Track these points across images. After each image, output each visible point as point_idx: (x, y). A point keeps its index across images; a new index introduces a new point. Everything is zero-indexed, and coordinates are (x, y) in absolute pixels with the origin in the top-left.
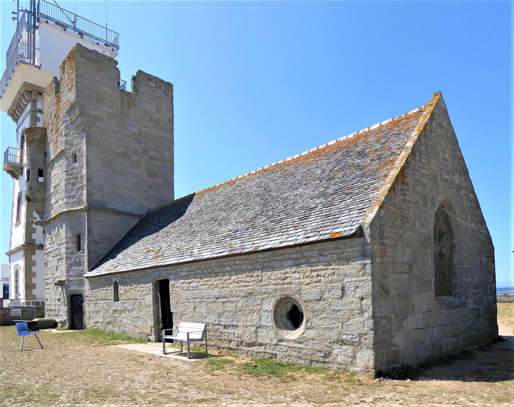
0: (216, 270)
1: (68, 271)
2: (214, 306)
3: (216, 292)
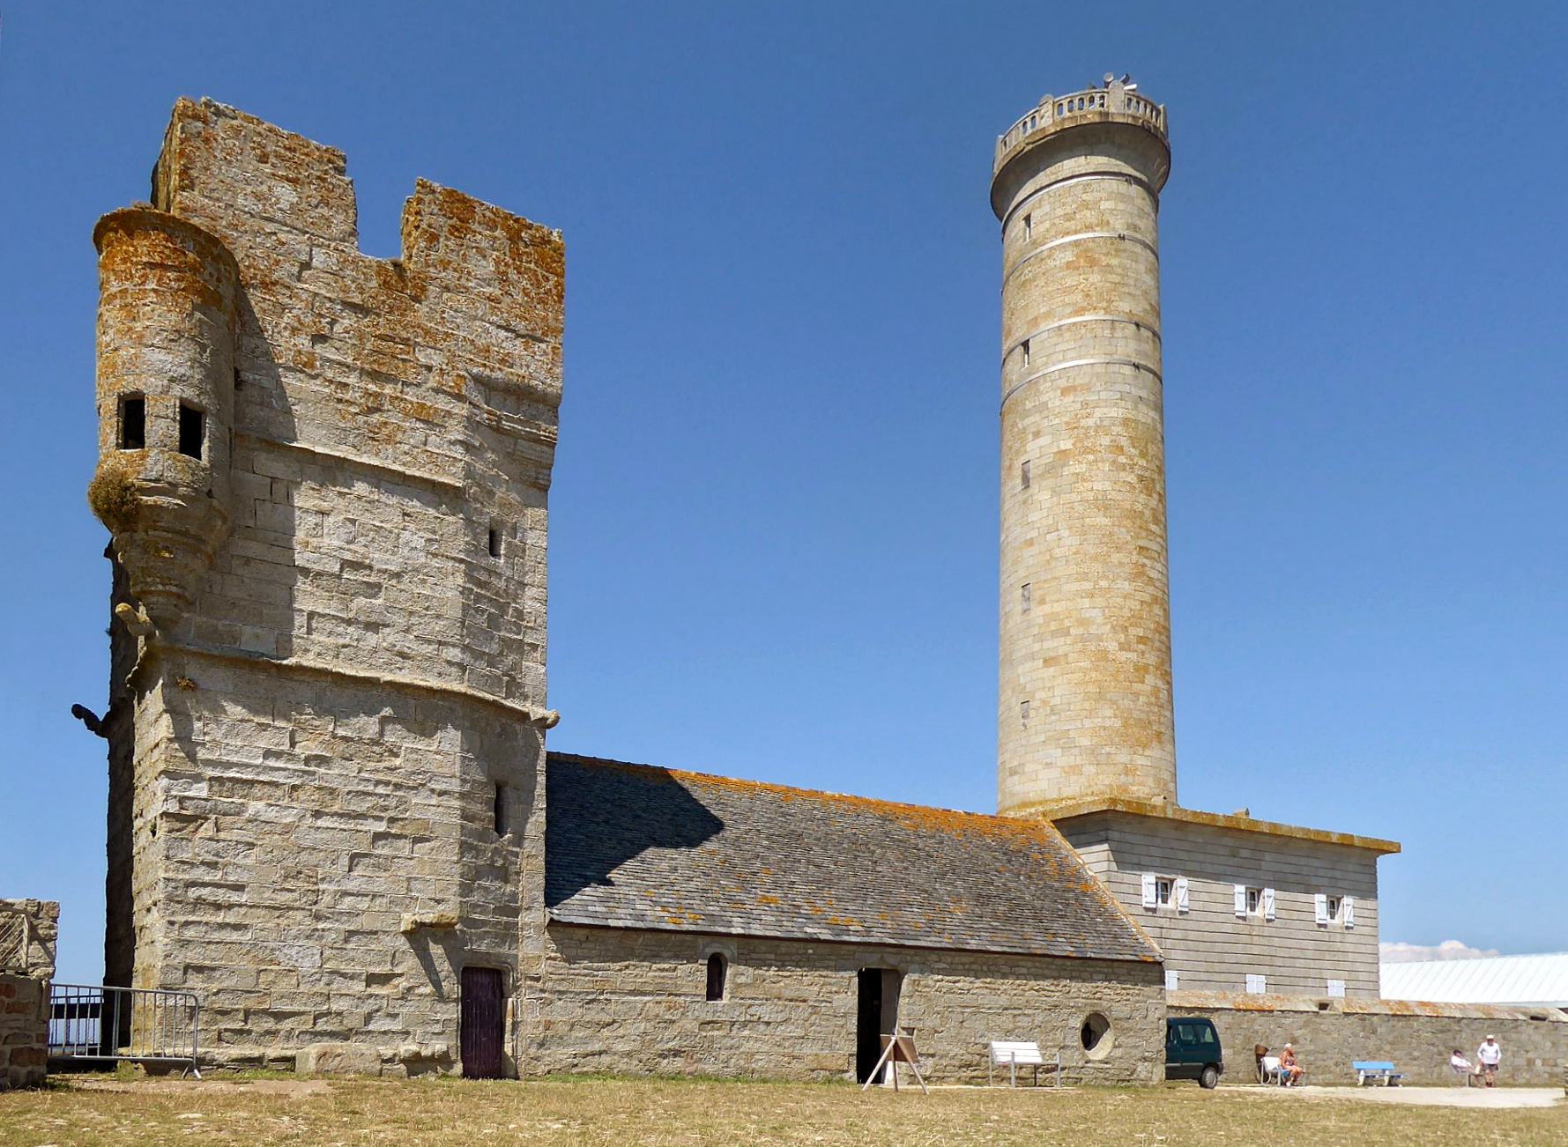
0: (1005, 969)
1: (465, 890)
3: (1003, 1000)
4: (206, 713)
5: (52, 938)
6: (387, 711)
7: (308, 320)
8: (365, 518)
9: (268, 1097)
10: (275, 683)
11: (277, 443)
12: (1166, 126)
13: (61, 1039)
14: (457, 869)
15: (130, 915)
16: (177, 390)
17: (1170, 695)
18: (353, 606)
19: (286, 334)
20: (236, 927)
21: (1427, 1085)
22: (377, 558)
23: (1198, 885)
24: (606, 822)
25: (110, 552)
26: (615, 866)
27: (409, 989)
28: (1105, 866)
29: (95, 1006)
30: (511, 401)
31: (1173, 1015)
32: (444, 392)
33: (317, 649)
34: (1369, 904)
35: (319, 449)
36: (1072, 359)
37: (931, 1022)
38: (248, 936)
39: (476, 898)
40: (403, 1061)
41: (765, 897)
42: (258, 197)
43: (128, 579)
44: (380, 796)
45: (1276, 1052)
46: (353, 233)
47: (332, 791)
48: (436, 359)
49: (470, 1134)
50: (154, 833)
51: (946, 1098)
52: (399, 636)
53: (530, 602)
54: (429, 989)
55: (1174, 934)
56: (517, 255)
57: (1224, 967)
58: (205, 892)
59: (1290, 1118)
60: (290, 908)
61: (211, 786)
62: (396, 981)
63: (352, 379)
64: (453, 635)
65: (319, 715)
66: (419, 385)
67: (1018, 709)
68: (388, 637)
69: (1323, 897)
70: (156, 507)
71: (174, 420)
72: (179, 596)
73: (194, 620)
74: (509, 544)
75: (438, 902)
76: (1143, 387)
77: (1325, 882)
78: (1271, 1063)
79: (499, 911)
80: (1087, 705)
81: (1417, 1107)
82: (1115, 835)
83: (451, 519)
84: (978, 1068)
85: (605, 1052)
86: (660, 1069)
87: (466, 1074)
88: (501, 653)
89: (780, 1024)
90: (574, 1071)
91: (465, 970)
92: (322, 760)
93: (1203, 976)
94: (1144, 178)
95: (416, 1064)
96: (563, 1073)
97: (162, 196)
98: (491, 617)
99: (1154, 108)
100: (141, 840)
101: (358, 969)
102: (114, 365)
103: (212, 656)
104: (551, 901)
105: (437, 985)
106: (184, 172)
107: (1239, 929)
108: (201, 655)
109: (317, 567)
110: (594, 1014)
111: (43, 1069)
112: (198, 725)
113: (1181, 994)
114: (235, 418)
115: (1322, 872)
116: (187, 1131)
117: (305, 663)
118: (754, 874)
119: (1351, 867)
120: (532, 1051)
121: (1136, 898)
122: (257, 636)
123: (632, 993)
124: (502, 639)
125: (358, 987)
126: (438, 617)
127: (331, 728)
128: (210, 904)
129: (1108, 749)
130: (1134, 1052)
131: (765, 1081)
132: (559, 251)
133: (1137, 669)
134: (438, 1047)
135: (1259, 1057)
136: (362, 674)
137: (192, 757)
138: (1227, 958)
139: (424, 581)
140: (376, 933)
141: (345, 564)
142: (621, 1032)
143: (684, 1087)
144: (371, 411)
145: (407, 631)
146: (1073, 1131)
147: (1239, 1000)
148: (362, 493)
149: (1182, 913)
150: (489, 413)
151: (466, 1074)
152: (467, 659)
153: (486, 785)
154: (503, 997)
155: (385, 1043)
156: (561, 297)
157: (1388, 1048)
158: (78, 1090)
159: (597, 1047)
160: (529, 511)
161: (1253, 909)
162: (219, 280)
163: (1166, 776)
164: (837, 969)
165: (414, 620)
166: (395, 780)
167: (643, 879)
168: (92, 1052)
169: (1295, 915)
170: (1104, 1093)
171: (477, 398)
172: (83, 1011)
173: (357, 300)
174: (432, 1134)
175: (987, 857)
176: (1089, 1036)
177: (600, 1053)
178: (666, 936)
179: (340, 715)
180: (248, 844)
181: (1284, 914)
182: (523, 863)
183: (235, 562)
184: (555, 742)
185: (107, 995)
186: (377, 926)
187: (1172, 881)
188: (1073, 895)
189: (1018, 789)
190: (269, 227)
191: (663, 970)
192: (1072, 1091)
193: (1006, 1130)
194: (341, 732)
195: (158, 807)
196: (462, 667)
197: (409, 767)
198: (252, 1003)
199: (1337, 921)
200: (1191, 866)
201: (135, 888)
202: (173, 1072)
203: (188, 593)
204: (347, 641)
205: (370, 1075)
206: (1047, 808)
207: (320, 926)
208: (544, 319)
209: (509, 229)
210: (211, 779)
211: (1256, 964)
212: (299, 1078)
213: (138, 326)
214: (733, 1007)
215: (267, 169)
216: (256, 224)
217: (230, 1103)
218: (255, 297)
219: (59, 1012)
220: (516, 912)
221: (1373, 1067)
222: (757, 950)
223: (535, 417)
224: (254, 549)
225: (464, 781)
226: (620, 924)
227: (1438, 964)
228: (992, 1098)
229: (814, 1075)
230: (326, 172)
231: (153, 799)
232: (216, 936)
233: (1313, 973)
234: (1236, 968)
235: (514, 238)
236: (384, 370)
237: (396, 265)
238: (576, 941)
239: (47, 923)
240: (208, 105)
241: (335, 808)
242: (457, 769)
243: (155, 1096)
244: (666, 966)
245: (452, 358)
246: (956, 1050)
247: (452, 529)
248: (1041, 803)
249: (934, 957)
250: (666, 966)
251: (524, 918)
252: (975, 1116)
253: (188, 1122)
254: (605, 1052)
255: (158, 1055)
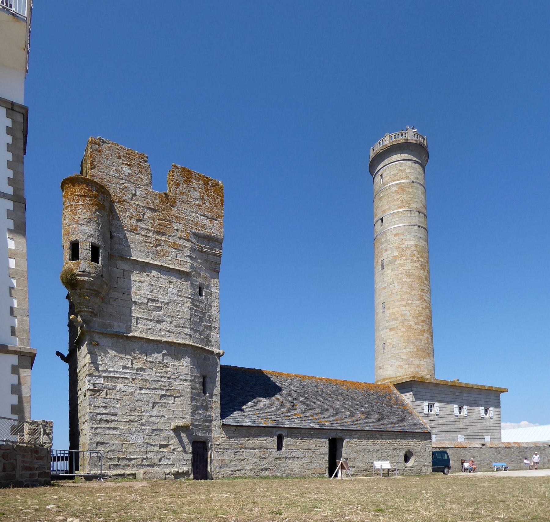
0: (378, 436)
1: (193, 414)
2: (376, 454)
3: (378, 447)
4: (102, 354)
5: (51, 434)
6: (165, 352)
7: (135, 214)
8: (156, 284)
9: (127, 488)
10: (125, 342)
11: (125, 258)
12: (427, 144)
13: (55, 469)
14: (190, 407)
15: (78, 425)
16: (90, 239)
17: (432, 340)
18: (152, 315)
19: (128, 219)
20: (114, 429)
21: (516, 470)
22: (160, 297)
23: (442, 405)
24: (241, 389)
25: (68, 297)
26: (244, 404)
27: (174, 449)
28: (411, 400)
29: (66, 457)
30: (206, 241)
31: (434, 450)
32: (183, 238)
33: (140, 330)
34: (498, 410)
35: (139, 260)
36: (397, 224)
37: (354, 455)
38: (118, 432)
39: (196, 417)
40: (173, 474)
41: (296, 414)
42: (117, 171)
43: (74, 307)
44: (163, 381)
45: (468, 461)
46: (150, 183)
47: (146, 380)
48: (180, 227)
49: (197, 499)
50: (85, 396)
51: (359, 481)
52: (168, 325)
53: (213, 312)
54: (181, 449)
55: (435, 422)
56: (207, 190)
57: (451, 433)
58: (103, 417)
59: (472, 484)
60: (132, 422)
61: (104, 379)
62: (169, 447)
63: (151, 235)
64: (187, 324)
65: (141, 353)
66: (174, 236)
67: (381, 346)
68: (165, 325)
69: (483, 408)
70: (83, 281)
71: (89, 250)
72: (92, 312)
73: (97, 321)
74: (206, 292)
75: (184, 418)
76: (421, 233)
77: (483, 403)
78: (466, 465)
79: (205, 421)
80: (404, 344)
81: (513, 477)
82: (414, 389)
83: (186, 283)
84: (370, 471)
85: (242, 469)
86: (261, 475)
87: (195, 478)
88: (204, 330)
89: (302, 458)
90: (232, 476)
91: (194, 442)
92: (142, 369)
93: (444, 436)
94: (420, 162)
95: (177, 475)
96: (228, 477)
97: (84, 171)
98: (200, 318)
99: (423, 138)
100: (81, 399)
101: (156, 443)
102: (68, 231)
103: (103, 334)
104: (223, 417)
105: (184, 447)
106: (92, 163)
107: (456, 420)
108: (100, 333)
109: (139, 301)
110: (238, 456)
111: (50, 479)
112: (99, 358)
113: (437, 443)
114: (110, 248)
115: (482, 400)
116: (99, 500)
117: (136, 335)
118: (293, 406)
119: (492, 397)
120: (217, 470)
121: (423, 411)
122: (119, 326)
123: (251, 449)
124: (204, 325)
125: (157, 449)
126: (182, 318)
127: (145, 358)
128: (105, 421)
129: (412, 359)
130: (421, 463)
131: (297, 478)
132: (221, 188)
133: (421, 331)
134: (185, 469)
135: (462, 463)
136: (156, 339)
137: (97, 369)
138: (452, 430)
139: (176, 305)
140: (162, 430)
141: (149, 300)
142: (248, 462)
143: (270, 481)
144: (157, 245)
145: (171, 323)
146: (402, 491)
147: (456, 444)
148: (155, 275)
149: (437, 415)
150: (198, 245)
151: (195, 478)
152: (192, 332)
153: (199, 377)
154: (207, 451)
155: (166, 468)
156: (222, 204)
157: (504, 458)
158: (62, 486)
159: (240, 468)
160: (213, 280)
161: (460, 413)
162: (104, 200)
163: (431, 368)
164: (321, 439)
165: (173, 319)
166: (168, 376)
167: (254, 409)
168: (66, 473)
169: (474, 414)
170: (412, 478)
171: (194, 240)
172: (63, 459)
173: (152, 206)
174: (183, 499)
175: (372, 398)
176: (407, 459)
177: (241, 470)
178: (263, 428)
179: (148, 353)
180: (117, 399)
181: (470, 414)
182: (212, 404)
183: (111, 300)
184: (223, 361)
185: (71, 453)
186: (163, 427)
187: (434, 404)
188: (401, 411)
189: (382, 374)
190: (121, 182)
191: (262, 440)
192: (401, 477)
193: (379, 492)
194: (149, 359)
195: (86, 387)
196: (190, 335)
197: (173, 371)
198: (120, 455)
199: (488, 416)
200: (440, 399)
201: (79, 416)
202: (94, 479)
203: (95, 310)
204: (150, 327)
205: (161, 479)
206: (392, 380)
207: (143, 428)
208: (217, 212)
209: (204, 181)
210: (104, 377)
211: (461, 432)
212: (137, 481)
213: (76, 217)
214: (286, 453)
215: (121, 161)
216: (116, 180)
217: (114, 490)
218: (117, 206)
219: (54, 459)
220: (210, 421)
221: (499, 465)
222: (294, 432)
223: (214, 247)
224: (117, 295)
225: (192, 376)
226: (247, 424)
227: (520, 429)
228: (374, 481)
229: (314, 475)
230: (141, 162)
231: (84, 384)
232: (107, 432)
233: (480, 434)
234: (455, 433)
235: (206, 184)
236: (162, 231)
237: (165, 194)
238: (232, 431)
239: (49, 428)
240: (100, 139)
241: (147, 386)
242: (189, 371)
243: (88, 488)
244: (263, 439)
245: (185, 226)
246: (362, 465)
247: (186, 287)
248: (389, 379)
249: (354, 433)
250: (263, 439)
251: (213, 423)
252: (369, 487)
253: (99, 497)
254: (242, 469)
255: (89, 474)
